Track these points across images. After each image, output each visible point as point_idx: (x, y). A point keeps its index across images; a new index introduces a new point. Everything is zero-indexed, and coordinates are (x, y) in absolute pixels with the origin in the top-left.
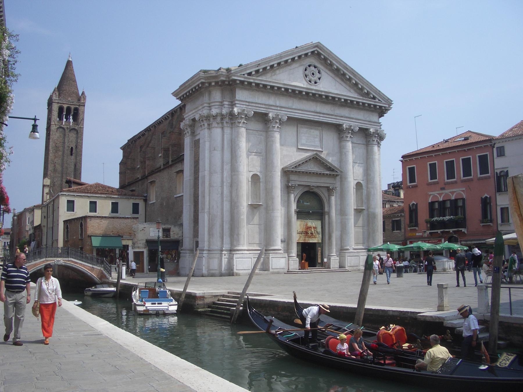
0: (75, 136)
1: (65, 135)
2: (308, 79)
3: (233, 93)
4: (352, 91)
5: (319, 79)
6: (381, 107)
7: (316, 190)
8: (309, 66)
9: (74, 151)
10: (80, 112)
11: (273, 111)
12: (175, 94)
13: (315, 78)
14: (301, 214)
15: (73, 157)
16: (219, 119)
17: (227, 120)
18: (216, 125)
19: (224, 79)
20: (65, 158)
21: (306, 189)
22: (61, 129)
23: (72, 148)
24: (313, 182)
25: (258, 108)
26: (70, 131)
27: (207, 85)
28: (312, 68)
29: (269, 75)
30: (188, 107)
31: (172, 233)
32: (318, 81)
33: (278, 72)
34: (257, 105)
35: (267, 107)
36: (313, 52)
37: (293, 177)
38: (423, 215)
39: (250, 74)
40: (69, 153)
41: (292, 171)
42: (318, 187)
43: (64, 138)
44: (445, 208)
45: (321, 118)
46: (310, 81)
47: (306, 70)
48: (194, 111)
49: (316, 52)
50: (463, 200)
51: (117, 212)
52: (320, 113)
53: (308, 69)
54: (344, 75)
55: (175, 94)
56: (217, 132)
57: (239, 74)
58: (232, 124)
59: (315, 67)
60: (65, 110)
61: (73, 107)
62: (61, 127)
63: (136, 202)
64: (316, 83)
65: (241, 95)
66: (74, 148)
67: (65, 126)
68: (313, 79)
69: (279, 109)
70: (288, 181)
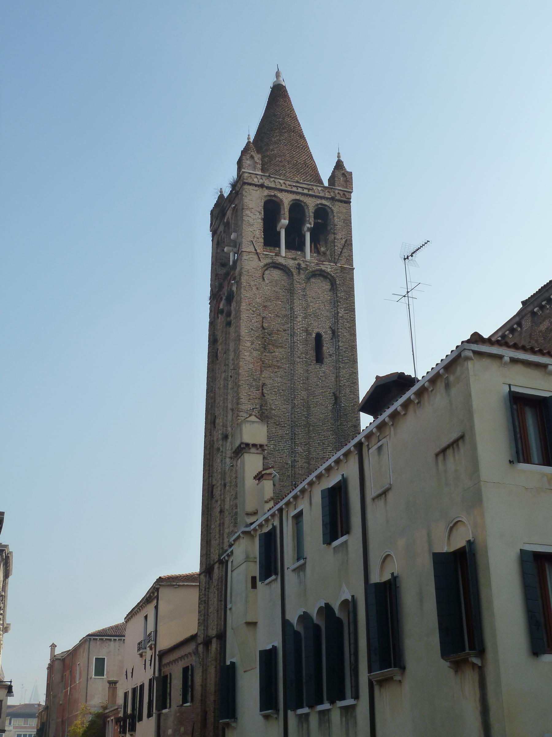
0: (327, 296)
9: (327, 348)
10: (337, 220)
15: (326, 368)
20: (300, 369)
22: (276, 274)
23: (319, 337)
26: (308, 279)
43: (292, 302)
62: (276, 266)
66: (326, 337)
67: (291, 263)
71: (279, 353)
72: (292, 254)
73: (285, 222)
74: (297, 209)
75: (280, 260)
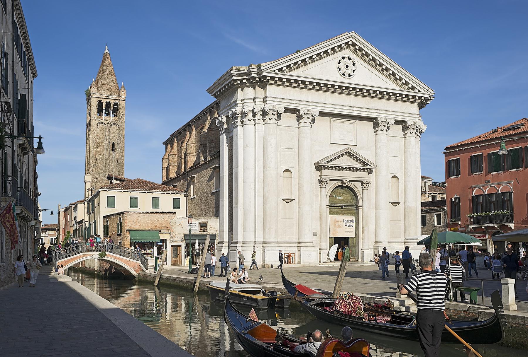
1: (106, 131)
2: (342, 72)
3: (264, 87)
4: (389, 81)
5: (354, 71)
6: (420, 98)
7: (349, 184)
8: (343, 58)
11: (305, 106)
12: (210, 91)
13: (349, 71)
14: (335, 208)
16: (250, 116)
17: (259, 116)
18: (249, 122)
19: (255, 75)
21: (340, 183)
23: (114, 143)
24: (346, 175)
25: (289, 104)
27: (239, 82)
28: (346, 60)
29: (301, 69)
30: (222, 105)
31: (208, 227)
32: (352, 74)
33: (310, 66)
34: (288, 101)
35: (299, 102)
36: (346, 43)
37: (325, 172)
38: (465, 208)
39: (280, 70)
40: (111, 148)
41: (324, 166)
42: (351, 181)
44: (490, 202)
45: (355, 112)
46: (344, 75)
47: (339, 63)
48: (227, 108)
49: (350, 43)
50: (511, 193)
51: (158, 207)
52: (354, 107)
53: (342, 61)
54: (381, 65)
55: (210, 91)
56: (250, 128)
57: (269, 71)
58: (264, 120)
59: (350, 59)
60: (104, 105)
61: (112, 102)
63: (177, 196)
64: (350, 76)
65: (272, 90)
68: (347, 72)
69: (311, 104)
70: (320, 176)
71: (101, 149)
72: (107, 118)
73: (104, 108)
74: (108, 105)
75: (102, 121)
